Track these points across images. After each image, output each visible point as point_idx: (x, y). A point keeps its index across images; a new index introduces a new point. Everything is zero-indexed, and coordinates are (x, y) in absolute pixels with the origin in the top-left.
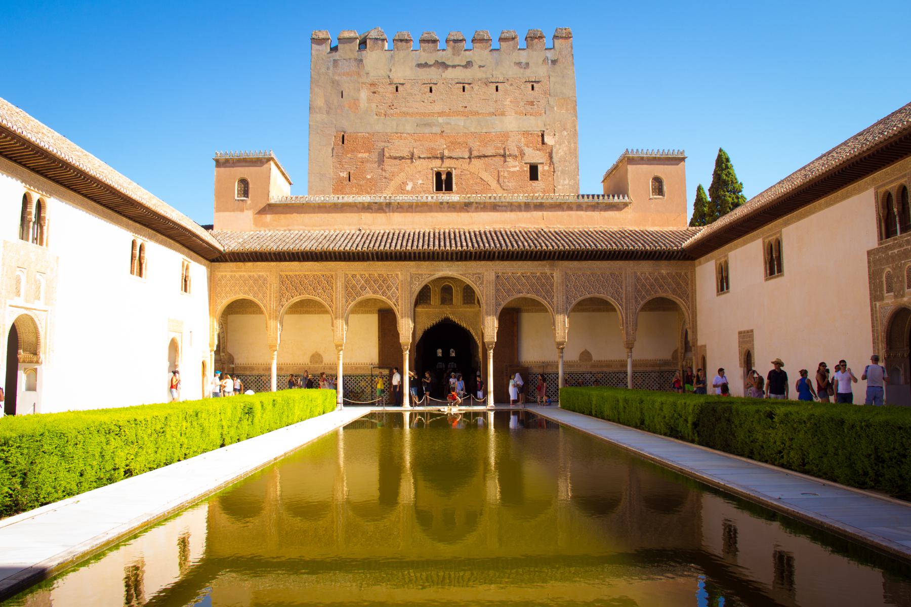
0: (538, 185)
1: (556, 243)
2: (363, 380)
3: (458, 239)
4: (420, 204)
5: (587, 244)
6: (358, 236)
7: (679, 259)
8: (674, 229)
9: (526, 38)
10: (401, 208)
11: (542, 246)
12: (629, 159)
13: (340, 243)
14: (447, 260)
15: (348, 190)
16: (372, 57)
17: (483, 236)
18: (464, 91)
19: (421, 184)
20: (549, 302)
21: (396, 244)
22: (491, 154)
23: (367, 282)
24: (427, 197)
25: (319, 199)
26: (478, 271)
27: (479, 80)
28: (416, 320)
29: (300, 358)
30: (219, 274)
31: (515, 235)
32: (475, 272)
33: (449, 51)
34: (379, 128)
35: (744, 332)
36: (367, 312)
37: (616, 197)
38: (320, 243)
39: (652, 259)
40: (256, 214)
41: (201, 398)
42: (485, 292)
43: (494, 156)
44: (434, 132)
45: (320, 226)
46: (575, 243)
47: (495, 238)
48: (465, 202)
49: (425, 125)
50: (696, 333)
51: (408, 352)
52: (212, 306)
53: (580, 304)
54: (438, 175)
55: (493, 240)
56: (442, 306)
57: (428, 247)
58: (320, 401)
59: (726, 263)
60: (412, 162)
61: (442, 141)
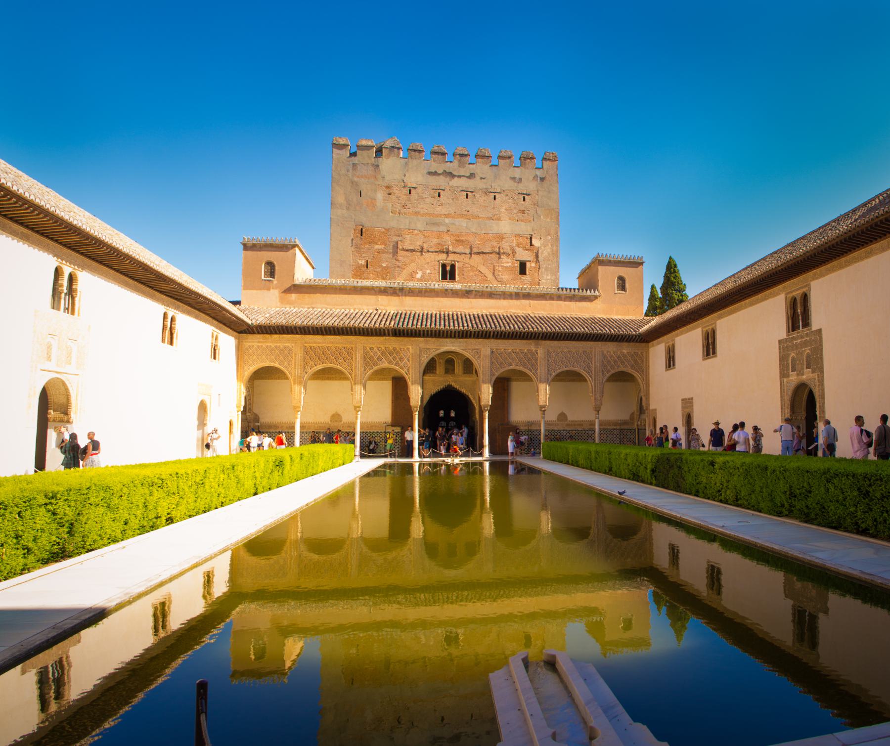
0: (526, 278)
1: (540, 326)
2: (378, 436)
3: (460, 320)
5: (565, 328)
6: (375, 314)
9: (521, 158)
10: (412, 292)
11: (529, 328)
13: (359, 320)
14: (451, 337)
15: (365, 275)
17: (481, 318)
20: (534, 374)
21: (408, 322)
22: (488, 251)
23: (384, 354)
24: (434, 285)
26: (477, 347)
27: (480, 189)
29: (321, 418)
31: (507, 318)
32: (473, 348)
33: (456, 163)
35: (686, 399)
36: (382, 379)
38: (341, 320)
40: (282, 293)
41: (228, 453)
42: (482, 364)
43: (491, 253)
45: (342, 305)
46: (555, 326)
47: (491, 321)
49: (434, 224)
51: (417, 413)
52: (239, 373)
54: (444, 266)
55: (489, 321)
56: (446, 375)
57: (435, 326)
58: (340, 455)
60: (422, 254)
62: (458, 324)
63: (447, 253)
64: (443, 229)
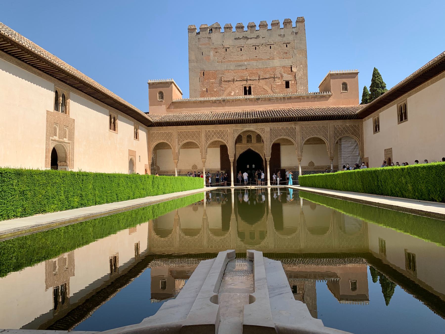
3: (253, 114)
4: (237, 100)
5: (311, 114)
7: (355, 119)
8: (353, 106)
9: (284, 23)
11: (290, 115)
12: (332, 76)
16: (215, 36)
18: (256, 49)
19: (238, 92)
20: (294, 140)
25: (194, 99)
28: (237, 150)
30: (152, 132)
33: (249, 31)
34: (219, 68)
36: (216, 147)
37: (325, 93)
39: (342, 119)
42: (266, 137)
44: (243, 69)
45: (195, 111)
46: (305, 113)
47: (270, 113)
48: (256, 98)
50: (364, 152)
53: (308, 140)
54: (245, 88)
55: (269, 114)
57: (240, 117)
59: (378, 118)
61: (247, 73)
62: (252, 116)
63: (247, 80)
64: (244, 68)
